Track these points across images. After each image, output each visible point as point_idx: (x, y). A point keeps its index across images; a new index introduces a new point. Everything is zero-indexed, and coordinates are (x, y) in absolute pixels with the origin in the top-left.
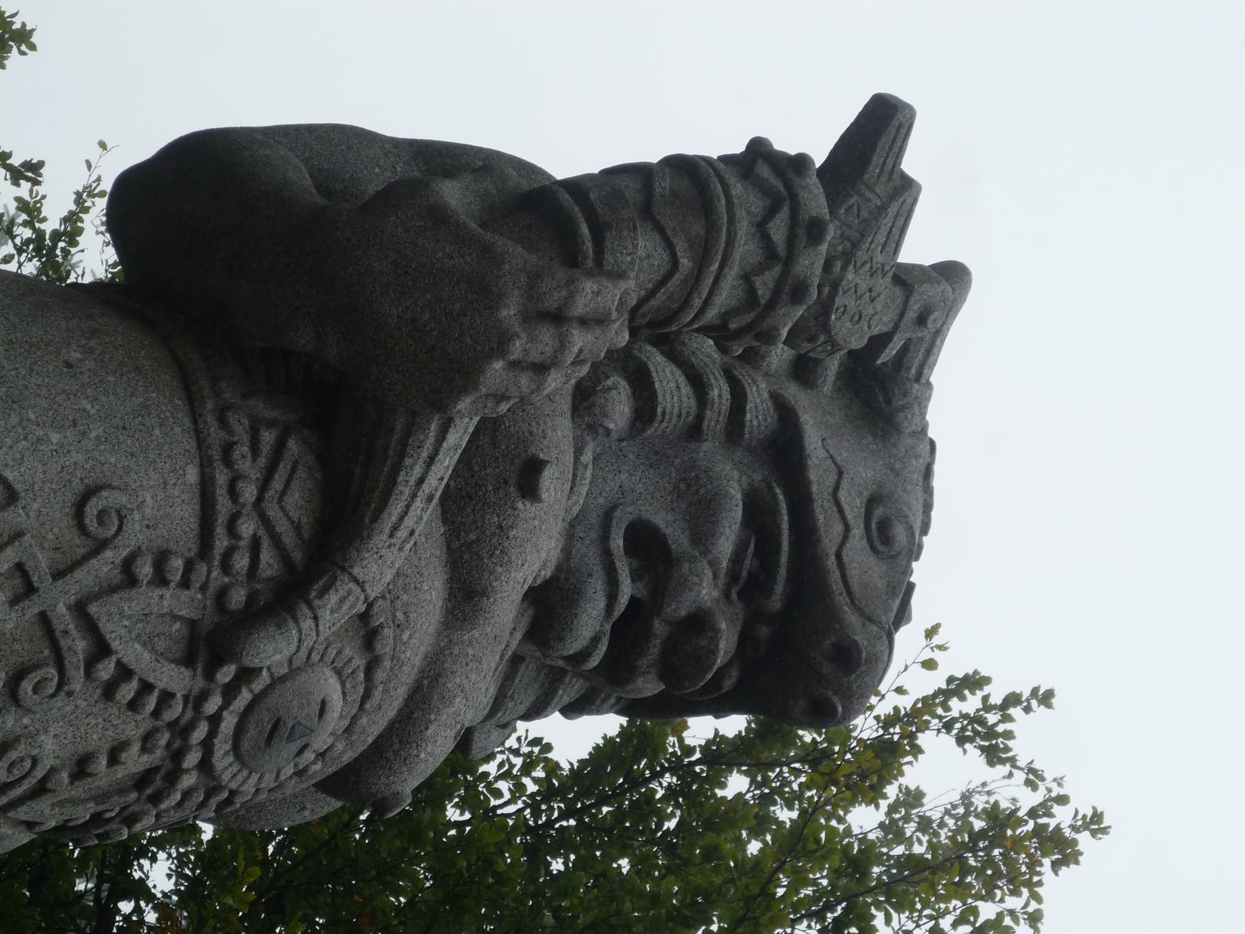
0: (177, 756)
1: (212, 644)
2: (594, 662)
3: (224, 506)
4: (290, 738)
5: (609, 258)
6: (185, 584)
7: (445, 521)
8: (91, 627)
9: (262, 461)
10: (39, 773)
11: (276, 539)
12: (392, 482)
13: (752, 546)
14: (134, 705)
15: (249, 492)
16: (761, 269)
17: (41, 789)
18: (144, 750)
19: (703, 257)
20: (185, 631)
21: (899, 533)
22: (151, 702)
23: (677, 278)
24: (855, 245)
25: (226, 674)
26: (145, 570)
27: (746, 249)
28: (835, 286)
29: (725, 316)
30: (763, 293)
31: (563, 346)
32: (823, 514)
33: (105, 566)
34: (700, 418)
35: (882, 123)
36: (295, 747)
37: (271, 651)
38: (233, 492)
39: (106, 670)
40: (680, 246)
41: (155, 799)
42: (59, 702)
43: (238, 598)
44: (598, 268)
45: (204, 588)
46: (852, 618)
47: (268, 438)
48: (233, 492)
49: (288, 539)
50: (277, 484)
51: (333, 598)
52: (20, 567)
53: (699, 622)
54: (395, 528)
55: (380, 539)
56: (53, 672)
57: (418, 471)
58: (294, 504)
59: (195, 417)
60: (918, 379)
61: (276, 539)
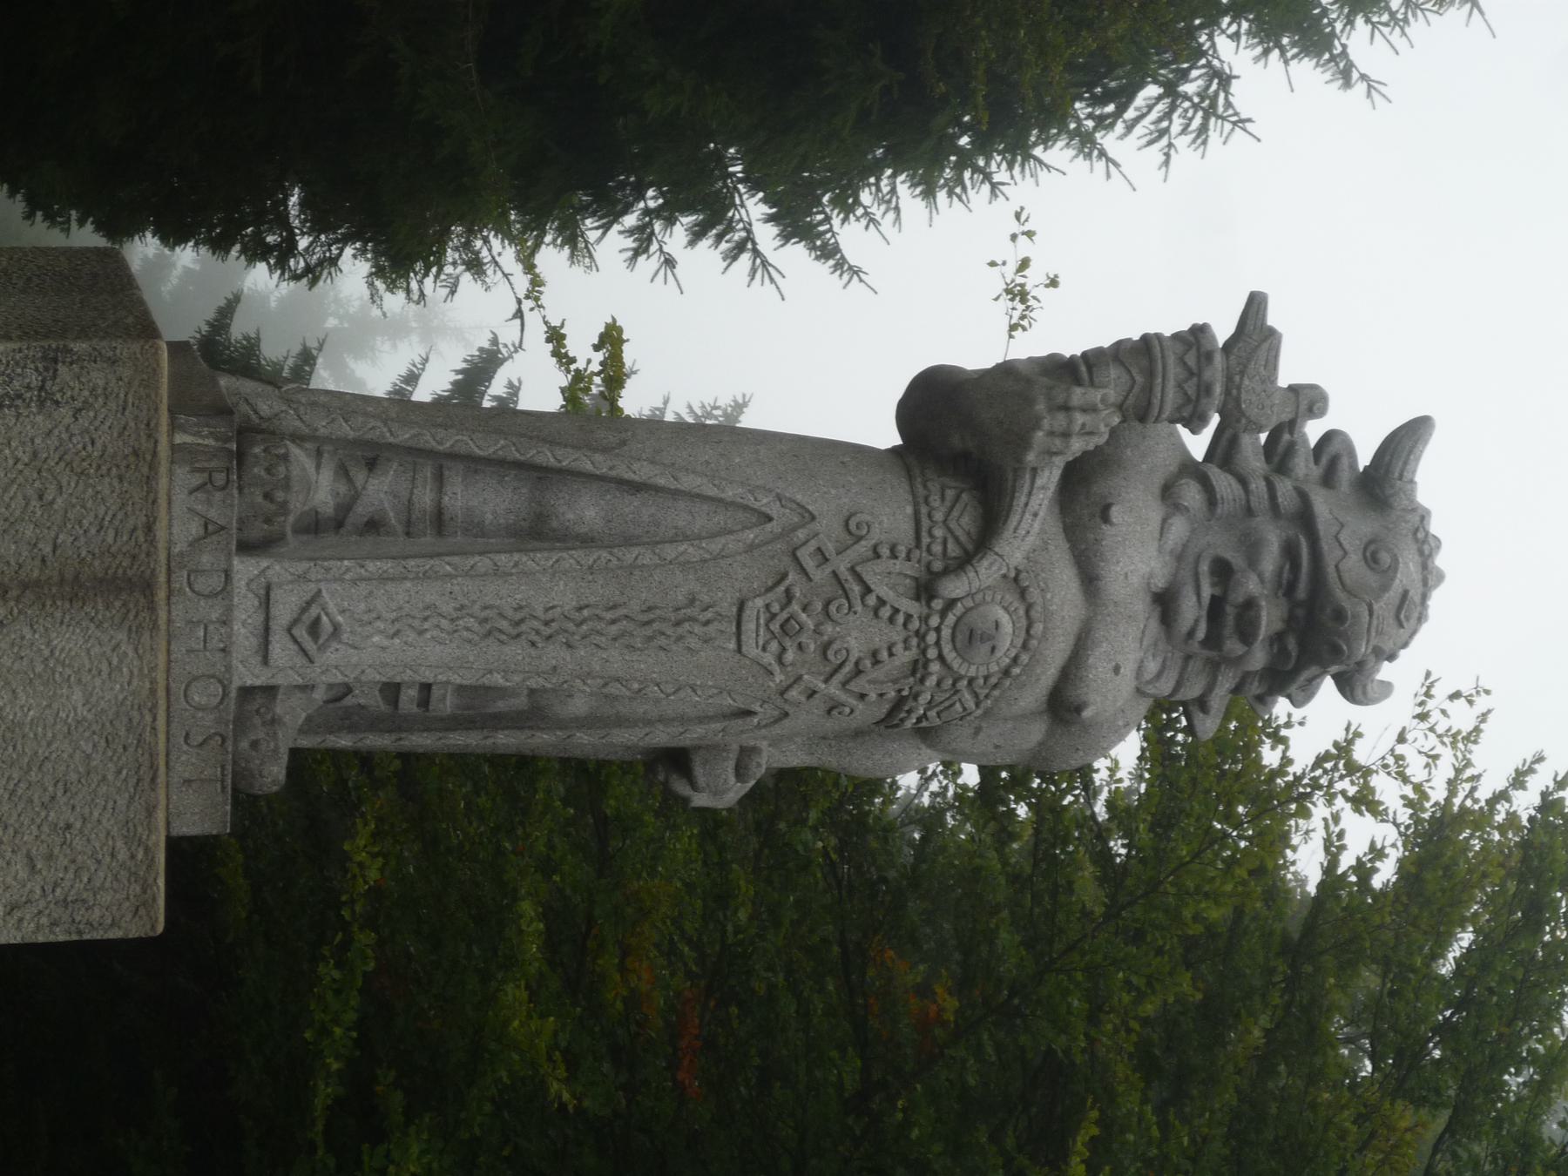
0: (924, 652)
1: (925, 590)
2: (1201, 634)
3: (925, 522)
4: (982, 640)
5: (1096, 380)
6: (908, 559)
7: (1069, 541)
8: (859, 579)
9: (948, 503)
10: (853, 659)
11: (957, 539)
12: (1011, 506)
13: (1287, 567)
14: (891, 620)
15: (939, 516)
16: (1186, 381)
17: (858, 672)
18: (906, 649)
19: (1150, 374)
20: (913, 584)
21: (1385, 558)
22: (900, 619)
23: (1136, 390)
24: (1245, 367)
25: (938, 604)
26: (885, 551)
27: (1174, 371)
28: (1239, 388)
29: (1179, 409)
30: (1191, 391)
31: (1071, 422)
32: (1326, 545)
33: (863, 548)
34: (1248, 501)
35: (1255, 304)
36: (986, 647)
37: (953, 587)
38: (930, 516)
39: (871, 600)
40: (1135, 372)
41: (922, 681)
42: (851, 617)
43: (938, 566)
44: (1092, 384)
45: (919, 561)
46: (1340, 595)
47: (950, 493)
48: (930, 516)
49: (963, 538)
50: (955, 513)
51: (985, 563)
52: (819, 549)
53: (1250, 604)
54: (1016, 529)
55: (1008, 533)
56: (844, 601)
57: (1023, 499)
58: (966, 522)
59: (912, 486)
60: (1400, 478)
61: (957, 539)
